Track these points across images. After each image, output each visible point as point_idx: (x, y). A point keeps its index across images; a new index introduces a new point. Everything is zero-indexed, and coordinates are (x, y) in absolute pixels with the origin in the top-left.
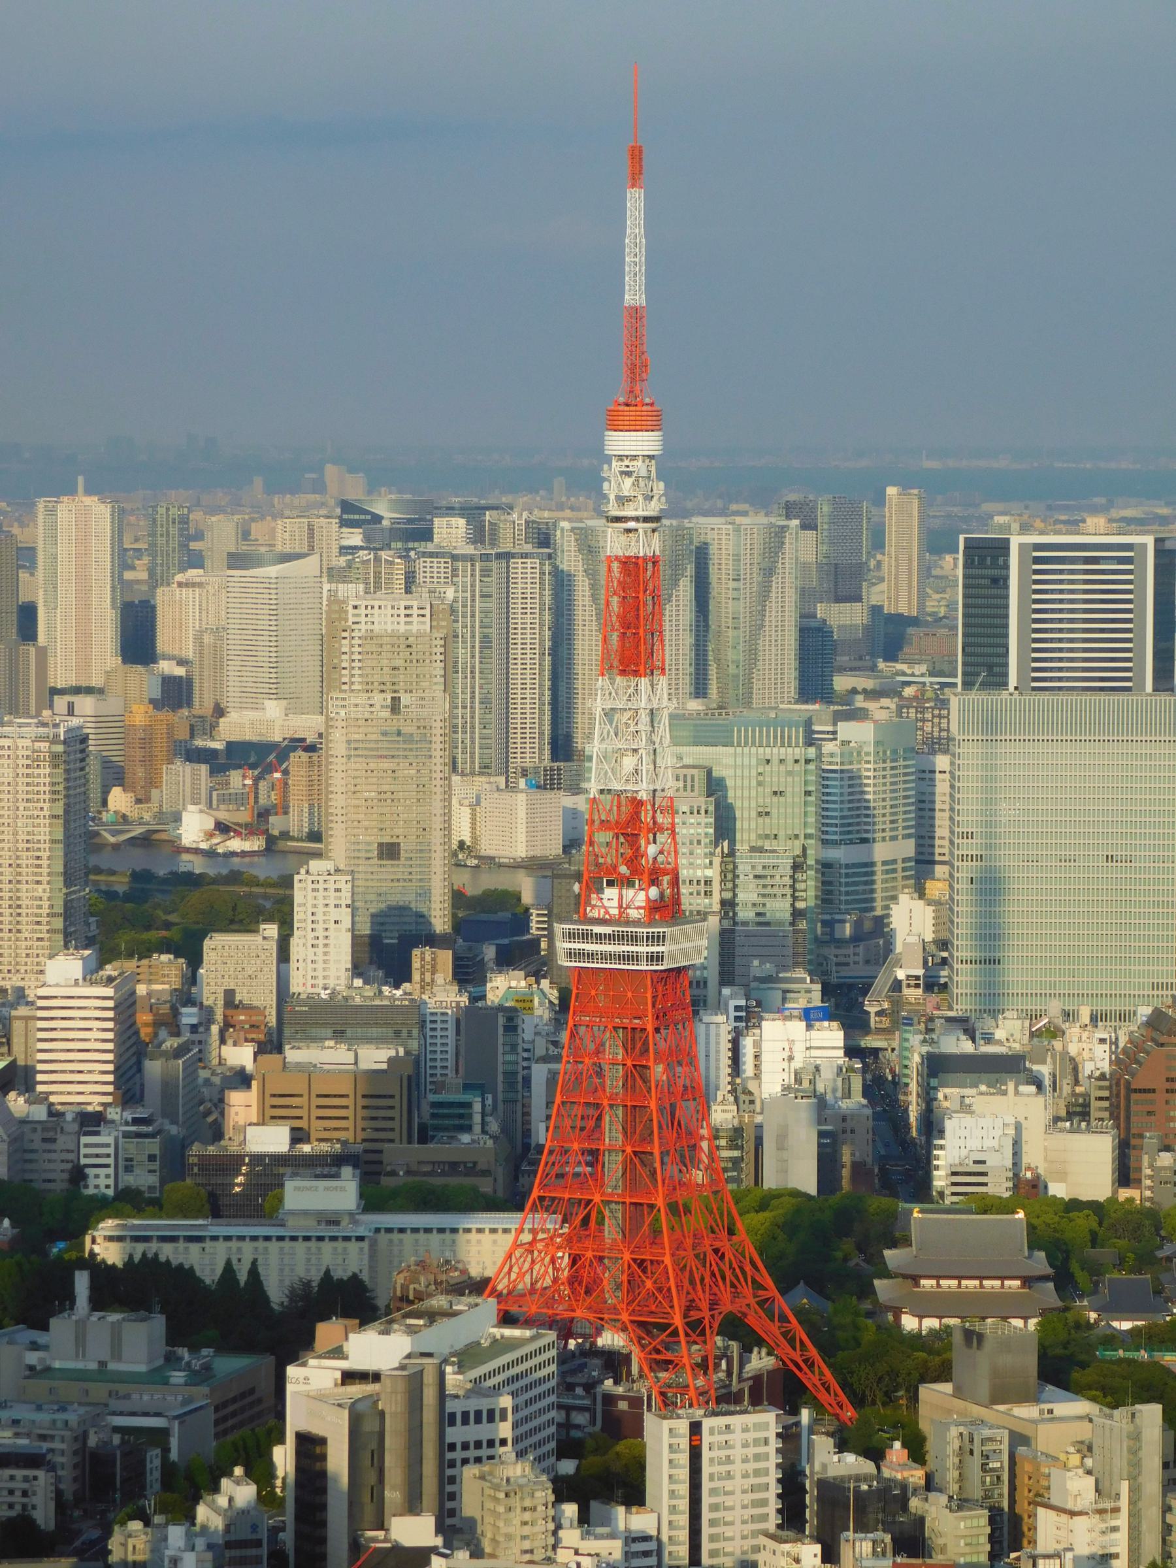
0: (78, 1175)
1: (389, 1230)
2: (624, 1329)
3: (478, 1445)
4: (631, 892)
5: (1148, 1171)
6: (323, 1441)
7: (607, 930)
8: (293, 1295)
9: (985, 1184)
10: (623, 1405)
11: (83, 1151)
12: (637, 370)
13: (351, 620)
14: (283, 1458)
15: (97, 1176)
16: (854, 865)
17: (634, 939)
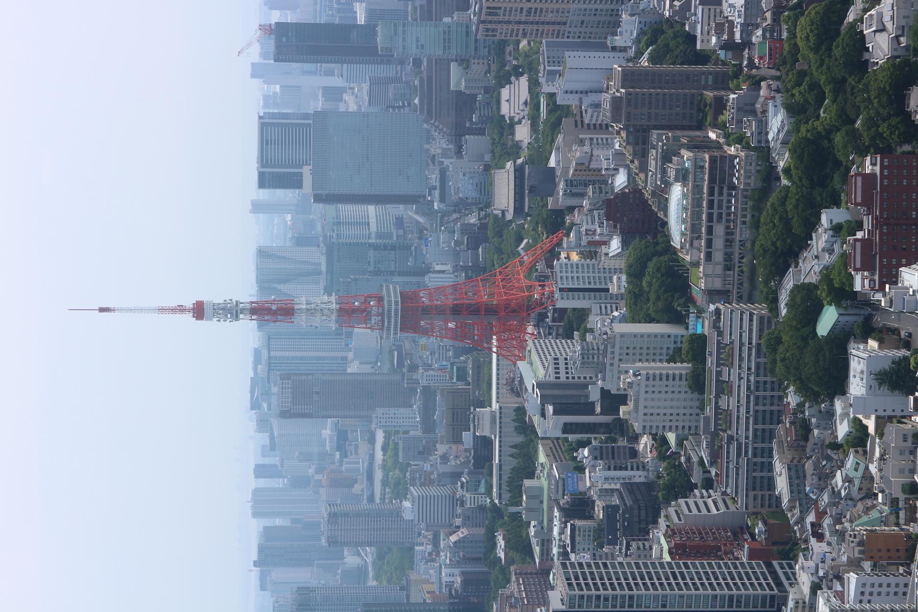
0: (482, 508)
1: (498, 398)
2: (529, 314)
3: (567, 368)
4: (373, 312)
5: (480, 125)
6: (565, 424)
7: (386, 320)
8: (519, 433)
9: (485, 183)
10: (556, 315)
11: (473, 506)
12: (181, 309)
13: (287, 409)
14: (572, 437)
15: (482, 501)
16: (377, 227)
17: (389, 311)
